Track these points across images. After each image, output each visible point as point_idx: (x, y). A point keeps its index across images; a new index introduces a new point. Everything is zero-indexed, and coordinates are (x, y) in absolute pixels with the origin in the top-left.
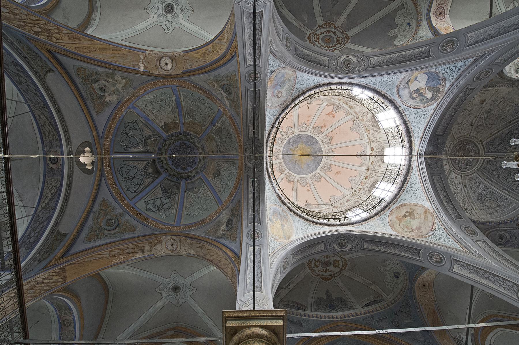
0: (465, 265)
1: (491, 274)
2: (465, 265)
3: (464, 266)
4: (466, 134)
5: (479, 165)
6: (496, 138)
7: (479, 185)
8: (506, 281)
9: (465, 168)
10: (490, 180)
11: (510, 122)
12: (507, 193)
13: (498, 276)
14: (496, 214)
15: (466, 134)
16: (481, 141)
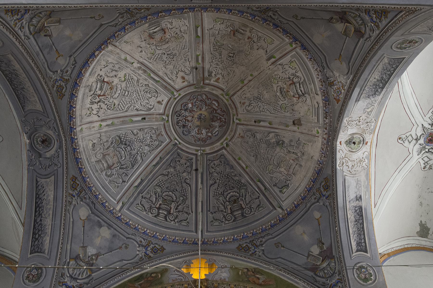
4: (240, 116)
5: (184, 146)
6: (232, 167)
7: (149, 145)
9: (178, 123)
10: (158, 163)
11: (260, 181)
12: (136, 184)
14: (93, 159)
15: (240, 116)
16: (227, 145)
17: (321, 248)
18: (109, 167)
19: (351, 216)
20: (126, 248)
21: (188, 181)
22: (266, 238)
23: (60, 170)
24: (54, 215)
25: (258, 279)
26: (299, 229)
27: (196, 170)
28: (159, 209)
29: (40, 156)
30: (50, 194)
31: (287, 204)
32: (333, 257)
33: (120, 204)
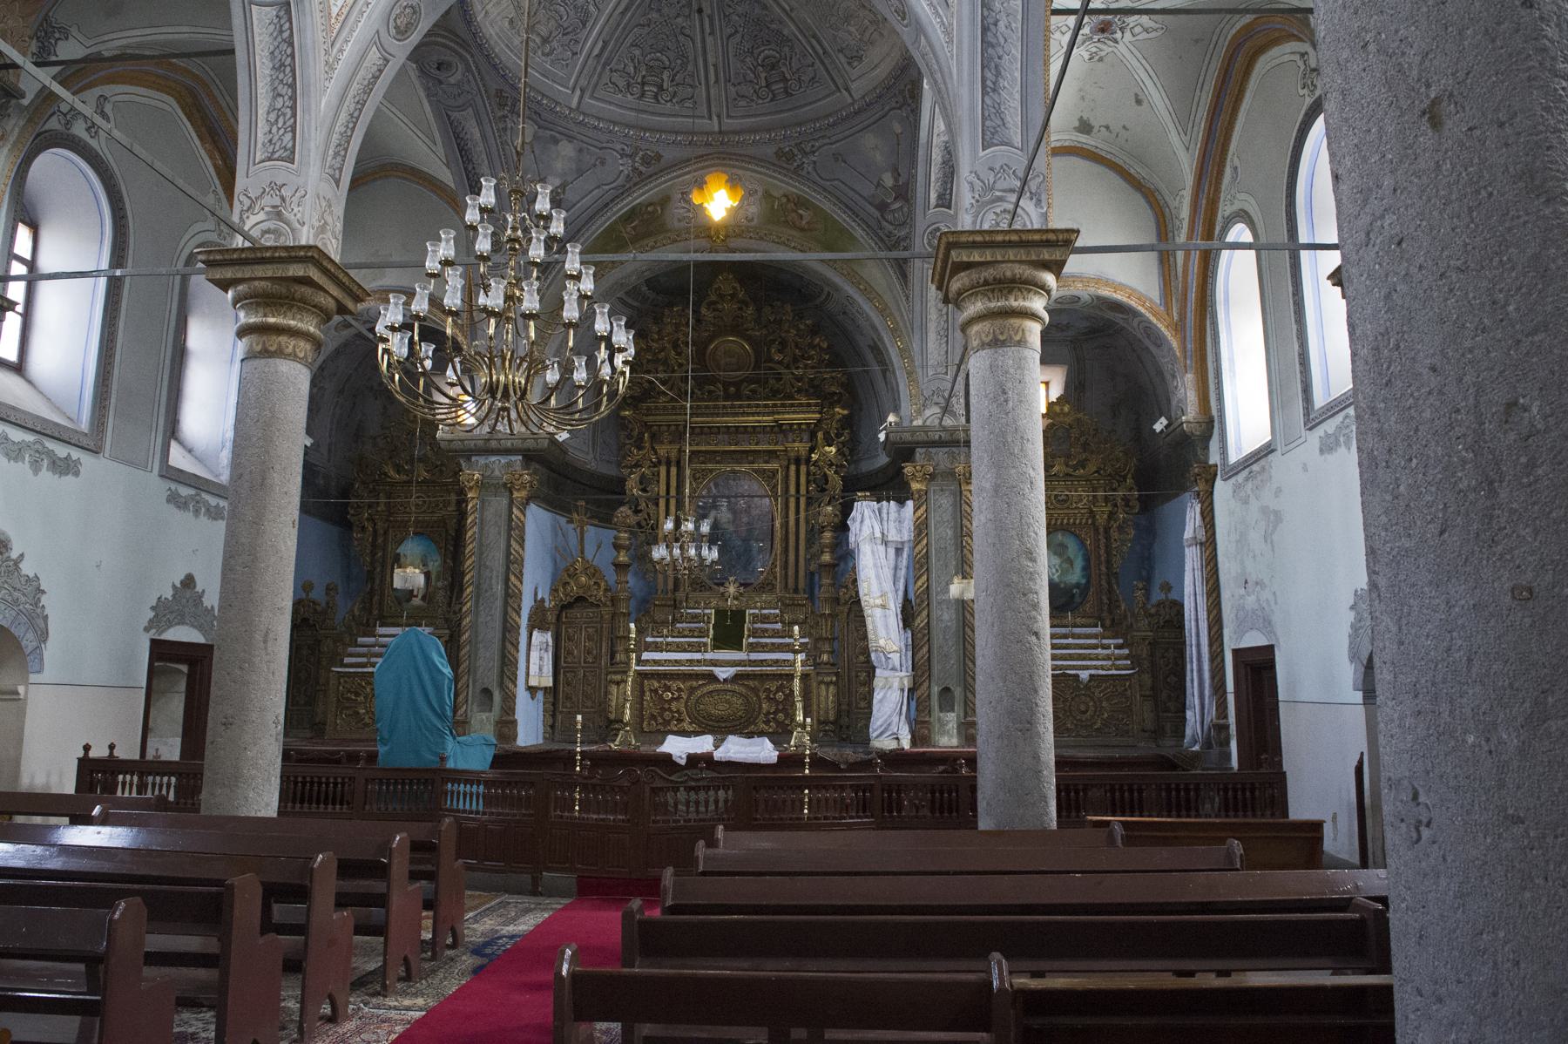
0: (286, 35)
1: (293, 98)
2: (286, 35)
3: (281, 32)
8: (289, 135)
11: (814, 36)
12: (596, 51)
13: (294, 115)
17: (896, 180)
18: (545, 41)
19: (937, 156)
20: (603, 163)
21: (687, 31)
22: (821, 142)
23: (478, 99)
24: (489, 155)
25: (801, 217)
26: (869, 140)
27: (700, 11)
28: (643, 84)
29: (441, 82)
30: (473, 131)
31: (859, 88)
32: (907, 201)
33: (578, 92)
